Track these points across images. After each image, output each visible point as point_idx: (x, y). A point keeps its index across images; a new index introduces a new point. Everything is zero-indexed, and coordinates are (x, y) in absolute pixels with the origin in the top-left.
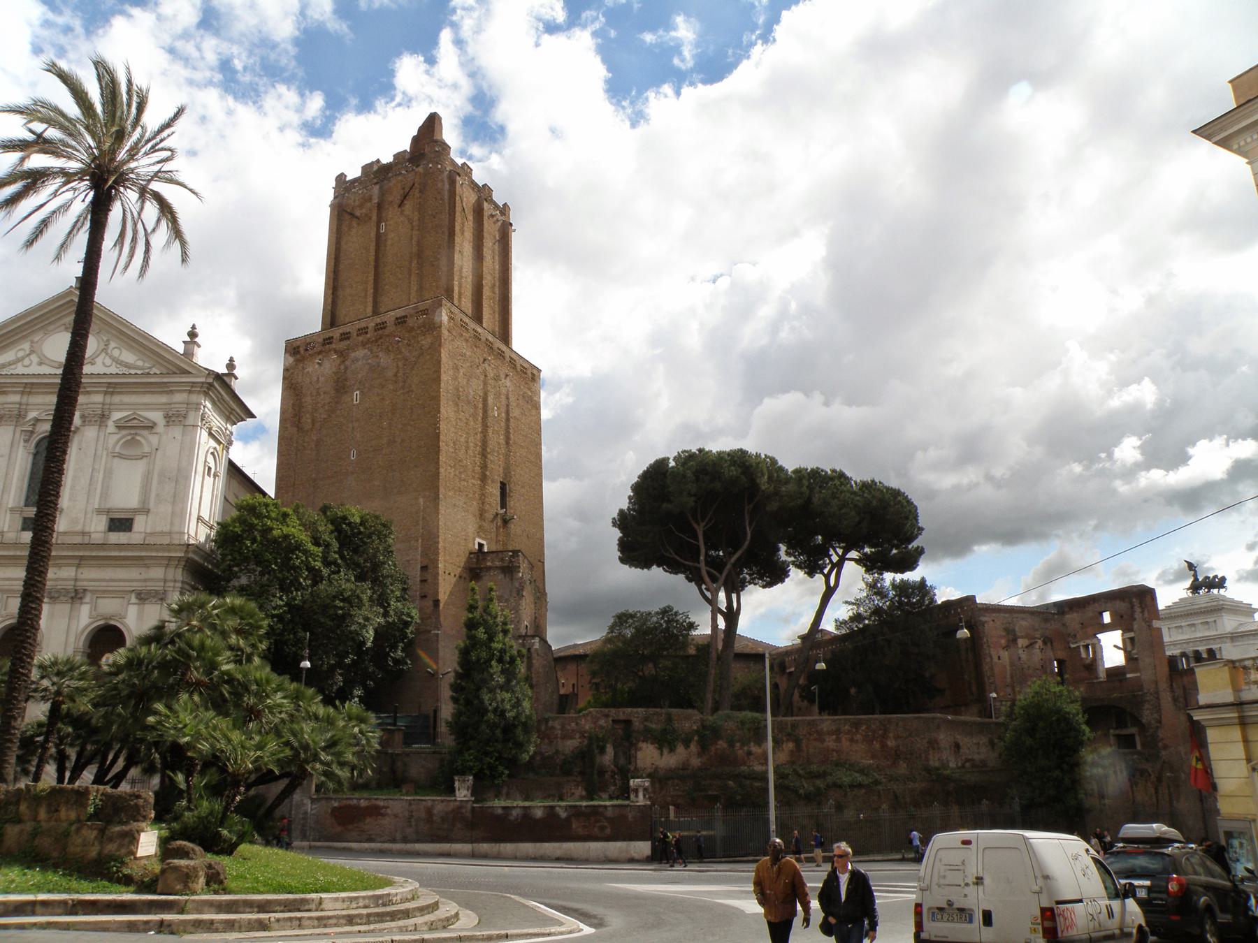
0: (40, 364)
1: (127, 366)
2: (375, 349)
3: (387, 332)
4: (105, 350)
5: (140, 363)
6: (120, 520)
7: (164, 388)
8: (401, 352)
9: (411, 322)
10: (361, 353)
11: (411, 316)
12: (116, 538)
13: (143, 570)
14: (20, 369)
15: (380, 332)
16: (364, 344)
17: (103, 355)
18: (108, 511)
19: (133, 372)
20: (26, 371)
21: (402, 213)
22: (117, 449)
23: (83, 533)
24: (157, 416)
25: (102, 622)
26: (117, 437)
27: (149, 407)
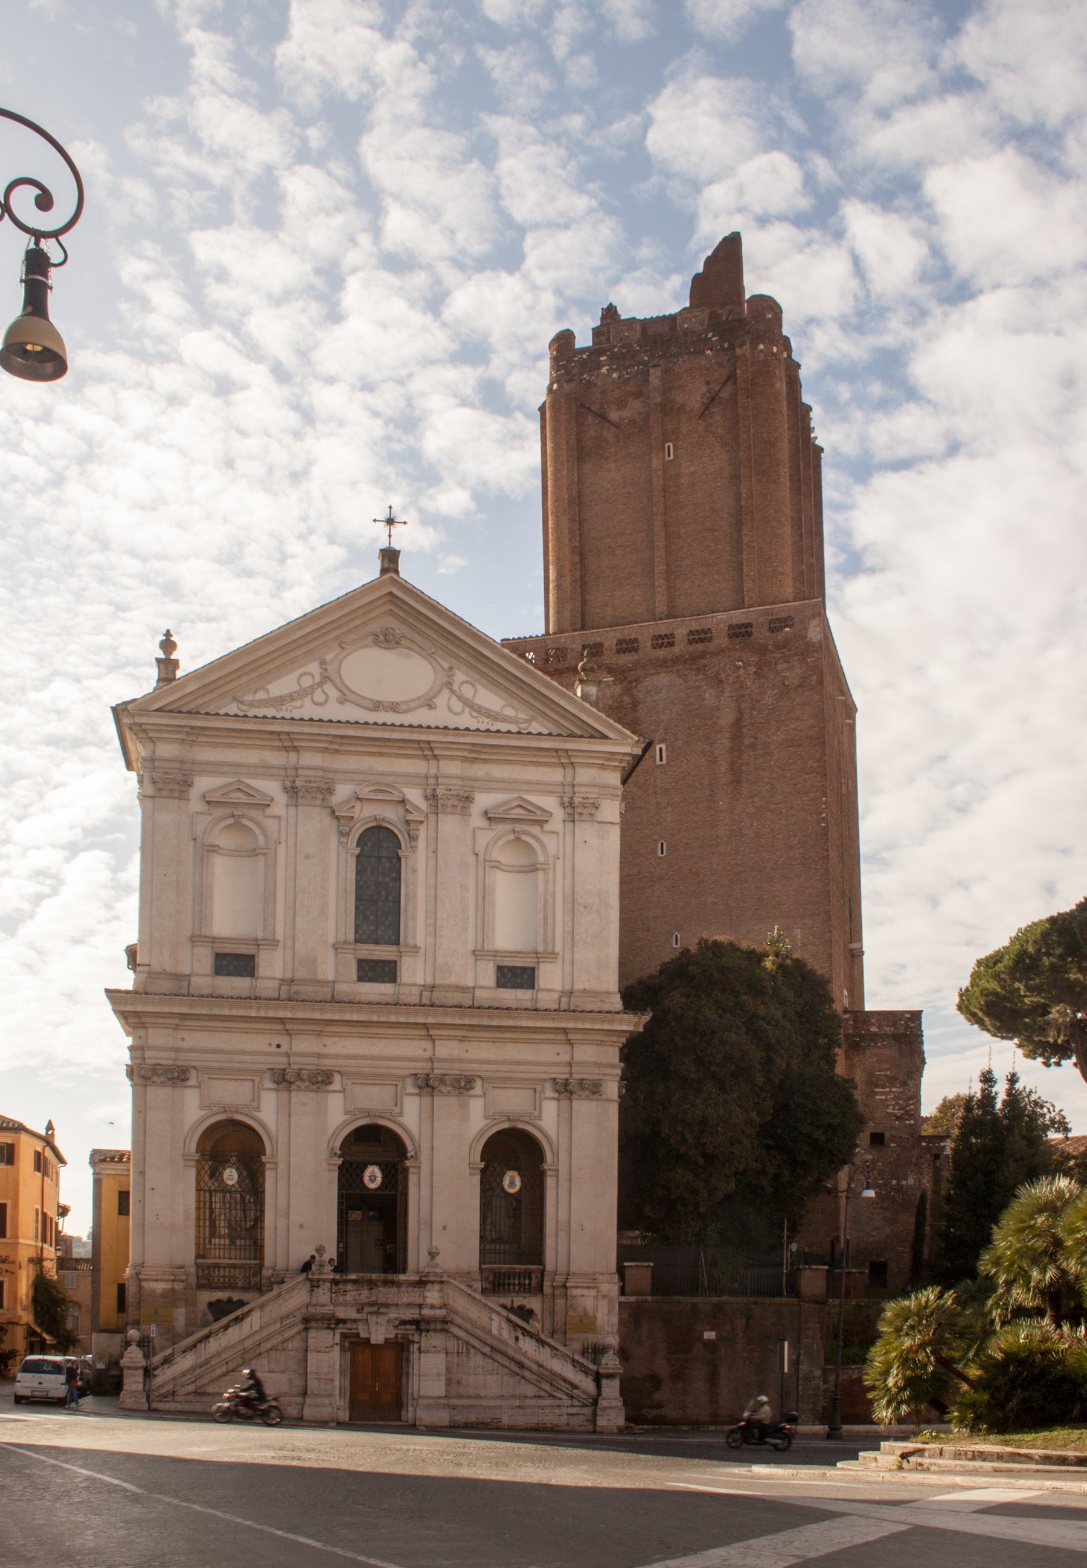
3: (712, 646)
6: (512, 969)
10: (663, 679)
14: (308, 710)
15: (700, 646)
19: (504, 727)
24: (549, 803)
25: (506, 1125)
26: (490, 835)
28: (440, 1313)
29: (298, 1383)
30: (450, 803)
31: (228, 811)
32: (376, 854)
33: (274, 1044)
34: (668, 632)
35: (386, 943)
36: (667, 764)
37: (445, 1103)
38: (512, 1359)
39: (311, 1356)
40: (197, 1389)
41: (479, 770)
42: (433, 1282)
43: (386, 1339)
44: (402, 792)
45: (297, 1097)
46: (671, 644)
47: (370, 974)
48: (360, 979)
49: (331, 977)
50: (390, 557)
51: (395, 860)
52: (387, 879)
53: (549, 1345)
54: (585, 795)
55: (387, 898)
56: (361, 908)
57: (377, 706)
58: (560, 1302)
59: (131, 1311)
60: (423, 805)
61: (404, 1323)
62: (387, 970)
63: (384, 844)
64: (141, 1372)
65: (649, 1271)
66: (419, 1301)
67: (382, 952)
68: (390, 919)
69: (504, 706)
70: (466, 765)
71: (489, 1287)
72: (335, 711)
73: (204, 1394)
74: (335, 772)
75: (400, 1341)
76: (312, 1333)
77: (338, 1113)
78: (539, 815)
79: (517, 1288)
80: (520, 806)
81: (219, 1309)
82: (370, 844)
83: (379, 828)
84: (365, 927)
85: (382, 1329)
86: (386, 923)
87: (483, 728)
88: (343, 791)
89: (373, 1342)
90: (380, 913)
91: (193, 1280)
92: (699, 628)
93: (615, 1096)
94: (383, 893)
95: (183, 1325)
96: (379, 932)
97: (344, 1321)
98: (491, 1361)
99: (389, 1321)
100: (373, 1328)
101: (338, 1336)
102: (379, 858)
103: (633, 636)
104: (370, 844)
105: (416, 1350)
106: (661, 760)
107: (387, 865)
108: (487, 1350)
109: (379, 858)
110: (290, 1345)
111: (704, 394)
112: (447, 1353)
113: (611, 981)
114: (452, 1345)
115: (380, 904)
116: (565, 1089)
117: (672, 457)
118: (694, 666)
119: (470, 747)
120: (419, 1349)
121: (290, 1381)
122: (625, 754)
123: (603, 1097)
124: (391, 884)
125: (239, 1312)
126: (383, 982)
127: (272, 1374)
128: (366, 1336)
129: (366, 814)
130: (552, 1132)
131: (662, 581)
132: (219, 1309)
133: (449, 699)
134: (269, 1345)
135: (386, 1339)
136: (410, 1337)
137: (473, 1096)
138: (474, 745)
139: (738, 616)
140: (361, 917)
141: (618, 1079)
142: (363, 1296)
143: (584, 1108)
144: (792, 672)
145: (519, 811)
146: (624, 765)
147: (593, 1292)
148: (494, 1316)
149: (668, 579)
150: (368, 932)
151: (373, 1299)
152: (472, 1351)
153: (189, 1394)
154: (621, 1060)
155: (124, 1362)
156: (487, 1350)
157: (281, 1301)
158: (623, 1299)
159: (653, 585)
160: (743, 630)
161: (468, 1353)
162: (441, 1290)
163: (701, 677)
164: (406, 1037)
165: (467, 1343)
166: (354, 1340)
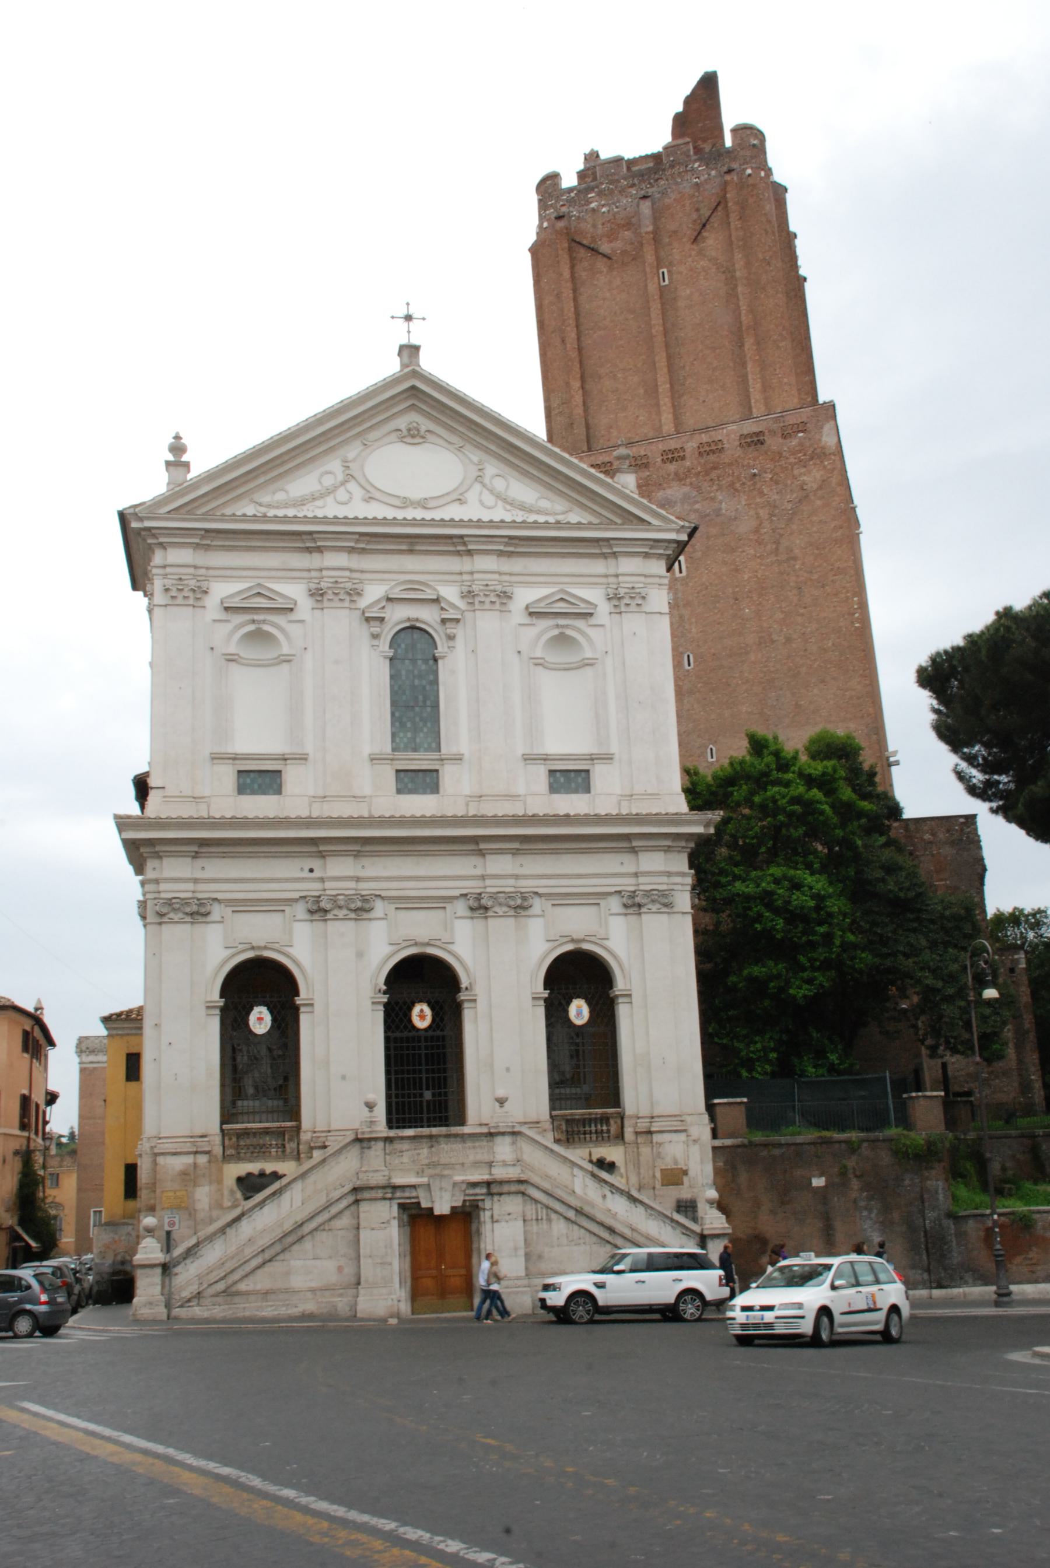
0: (369, 499)
1: (523, 507)
2: (705, 486)
3: (726, 458)
4: (479, 479)
5: (544, 504)
7: (603, 549)
8: (761, 493)
9: (773, 443)
11: (772, 432)
12: (259, 806)
13: (627, 858)
15: (712, 458)
16: (679, 478)
17: (477, 487)
18: (235, 758)
19: (541, 519)
20: (341, 512)
21: (701, 253)
22: (232, 649)
23: (196, 799)
24: (594, 595)
25: (569, 947)
27: (288, 574)
28: (513, 1173)
29: (349, 1270)
30: (487, 600)
31: (247, 617)
32: (410, 656)
33: (307, 869)
34: (678, 446)
35: (426, 750)
36: (688, 576)
37: (501, 926)
38: (601, 1224)
39: (363, 1234)
40: (228, 1287)
41: (517, 565)
42: (503, 1134)
43: (453, 1208)
44: (435, 590)
45: (334, 927)
46: (683, 458)
47: (410, 786)
48: (399, 791)
49: (367, 791)
50: (409, 351)
51: (431, 662)
52: (424, 682)
53: (641, 1202)
54: (630, 586)
55: (424, 702)
56: (397, 714)
57: (406, 503)
58: (645, 1151)
59: (143, 1194)
60: (461, 604)
61: (474, 1185)
62: (428, 780)
63: (419, 646)
64: (159, 1270)
65: (743, 1108)
66: (486, 1158)
67: (420, 761)
68: (429, 725)
69: (539, 498)
70: (503, 559)
71: (563, 1137)
72: (360, 509)
73: (238, 1293)
74: (362, 572)
75: (468, 1209)
76: (364, 1207)
77: (381, 945)
78: (583, 608)
79: (594, 1136)
80: (562, 599)
81: (250, 1185)
82: (403, 646)
83: (413, 628)
84: (401, 735)
85: (447, 1196)
86: (425, 730)
87: (519, 520)
88: (373, 592)
89: (437, 1212)
90: (417, 719)
91: (218, 1150)
92: (710, 440)
93: (689, 909)
94: (421, 698)
95: (207, 1207)
96: (418, 740)
97: (403, 1187)
98: (576, 1227)
99: (455, 1184)
100: (436, 1193)
101: (395, 1208)
102: (414, 661)
103: (643, 453)
104: (403, 646)
105: (488, 1220)
106: (681, 572)
107: (423, 667)
108: (571, 1214)
109: (414, 661)
110: (338, 1223)
111: (695, 221)
112: (524, 1221)
113: (675, 782)
114: (530, 1210)
115: (417, 709)
116: (633, 905)
117: (667, 282)
118: (708, 478)
119: (506, 540)
120: (492, 1216)
121: (340, 1269)
122: (669, 541)
123: (675, 910)
124: (428, 688)
125: (276, 1186)
126: (424, 793)
127: (318, 1262)
128: (429, 1205)
129: (398, 615)
130: (622, 954)
131: (667, 400)
132: (250, 1185)
133: (481, 493)
134: (313, 1225)
135: (453, 1208)
136: (480, 1204)
137: (529, 916)
138: (510, 538)
139: (749, 427)
140: (397, 724)
141: (689, 888)
142: (422, 1156)
143: (654, 922)
144: (812, 477)
145: (562, 604)
146: (669, 552)
147: (682, 1137)
148: (576, 1171)
149: (673, 398)
150: (405, 740)
151: (435, 1159)
152: (553, 1216)
153: (217, 1295)
154: (690, 868)
155: (139, 1257)
156: (571, 1214)
157: (327, 1168)
158: (718, 1143)
159: (658, 405)
160: (755, 439)
161: (549, 1220)
162: (514, 1143)
163: (715, 488)
164: (453, 853)
165: (547, 1207)
166: (414, 1212)
